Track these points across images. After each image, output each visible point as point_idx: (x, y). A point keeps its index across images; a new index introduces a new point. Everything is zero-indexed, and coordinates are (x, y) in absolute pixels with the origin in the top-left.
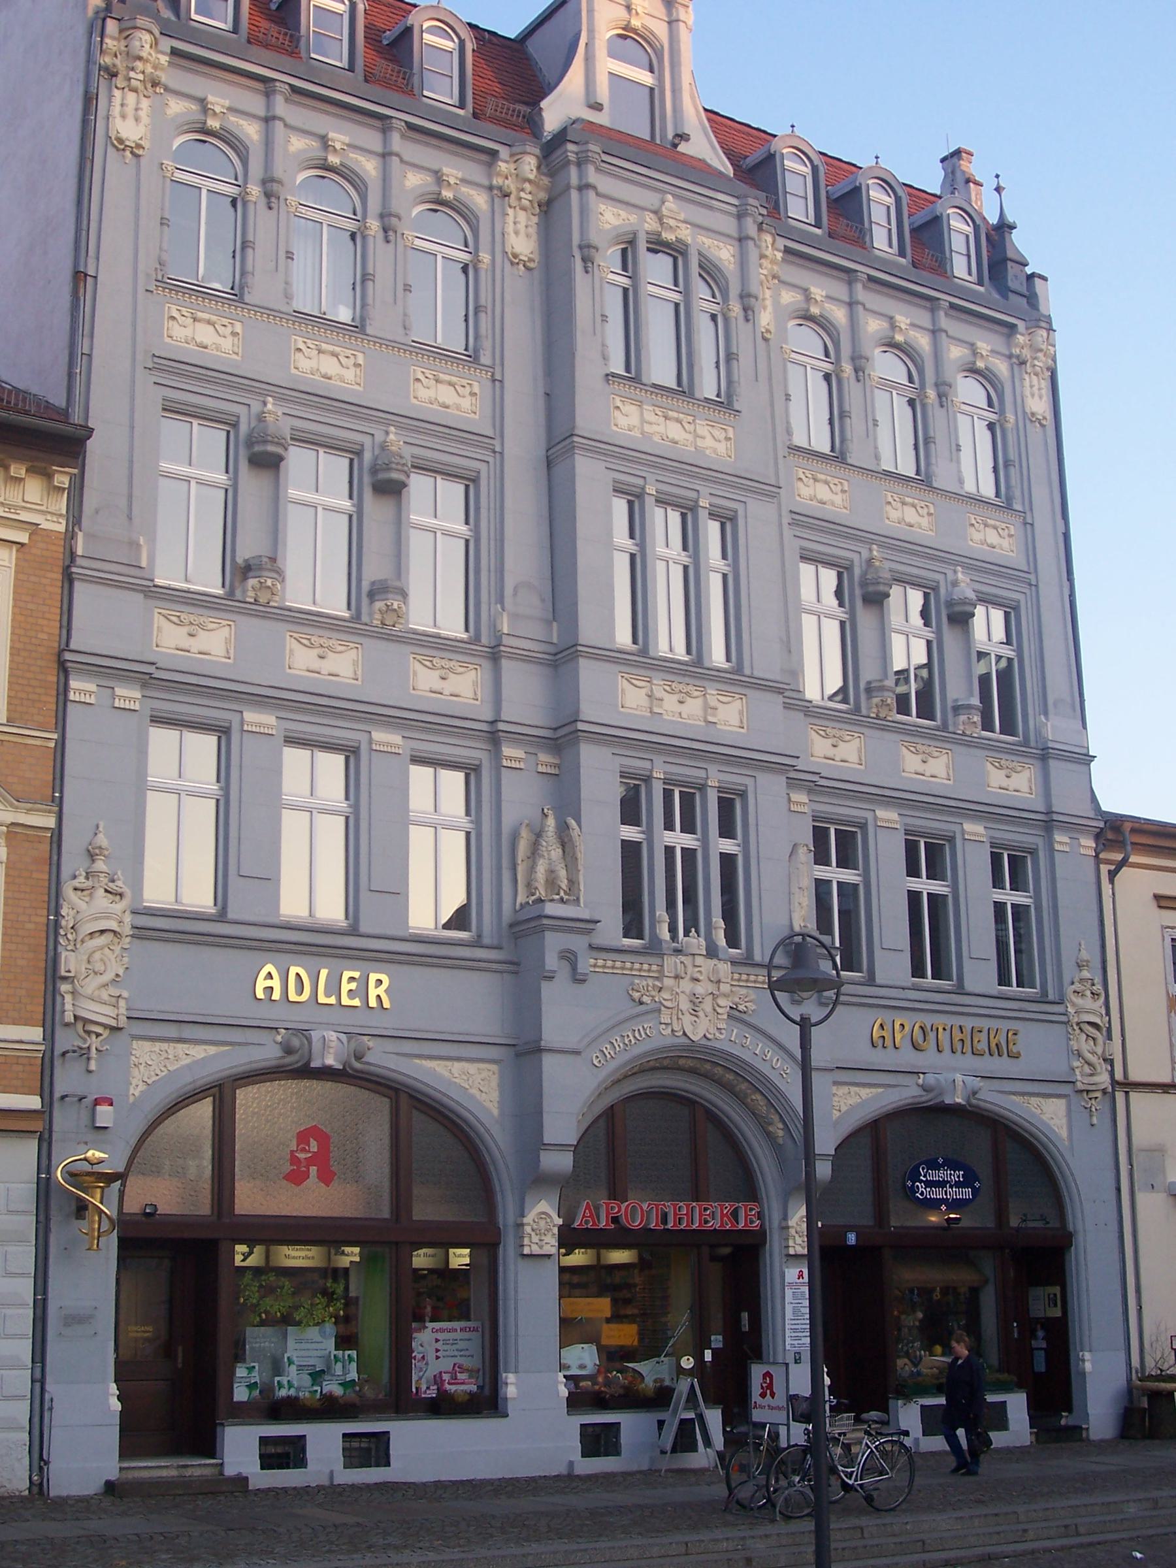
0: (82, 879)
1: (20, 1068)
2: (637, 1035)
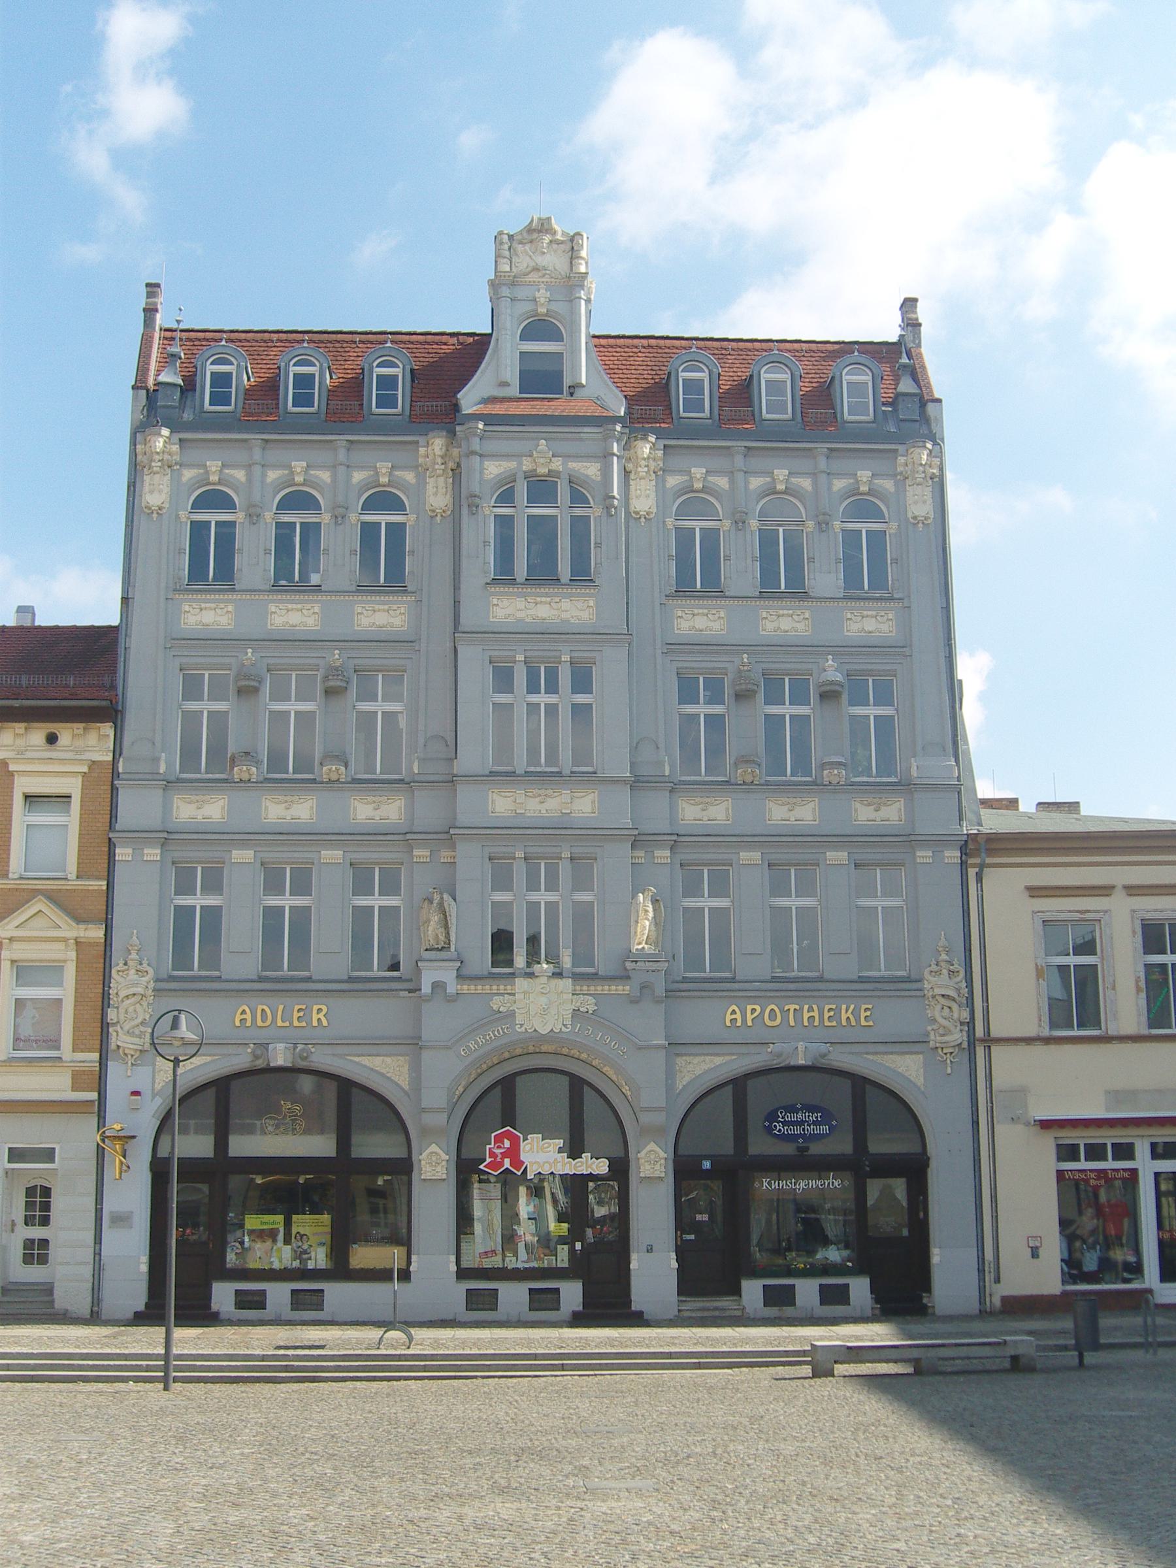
0: (121, 965)
1: (86, 1077)
2: (496, 1033)
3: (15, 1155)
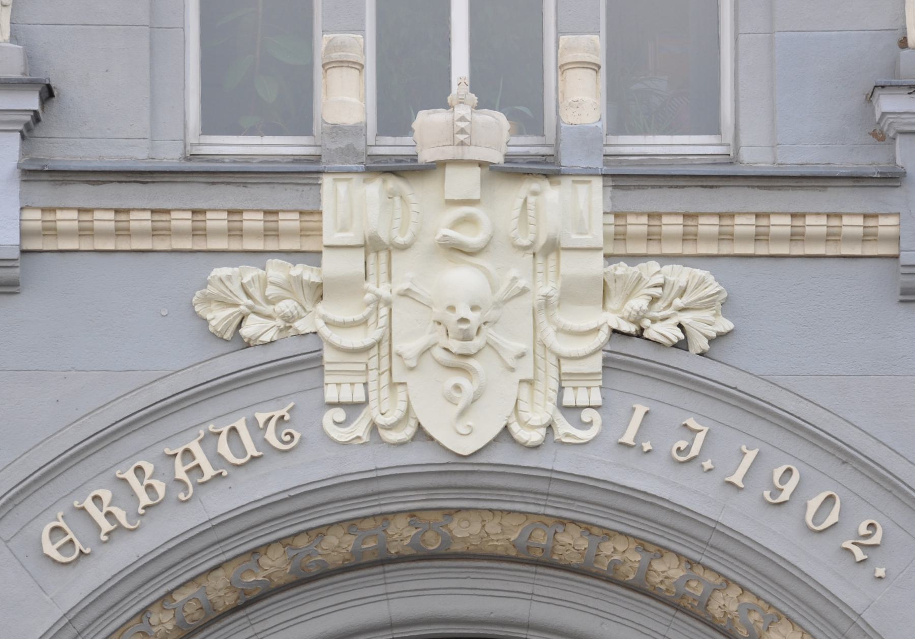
2: (223, 447)
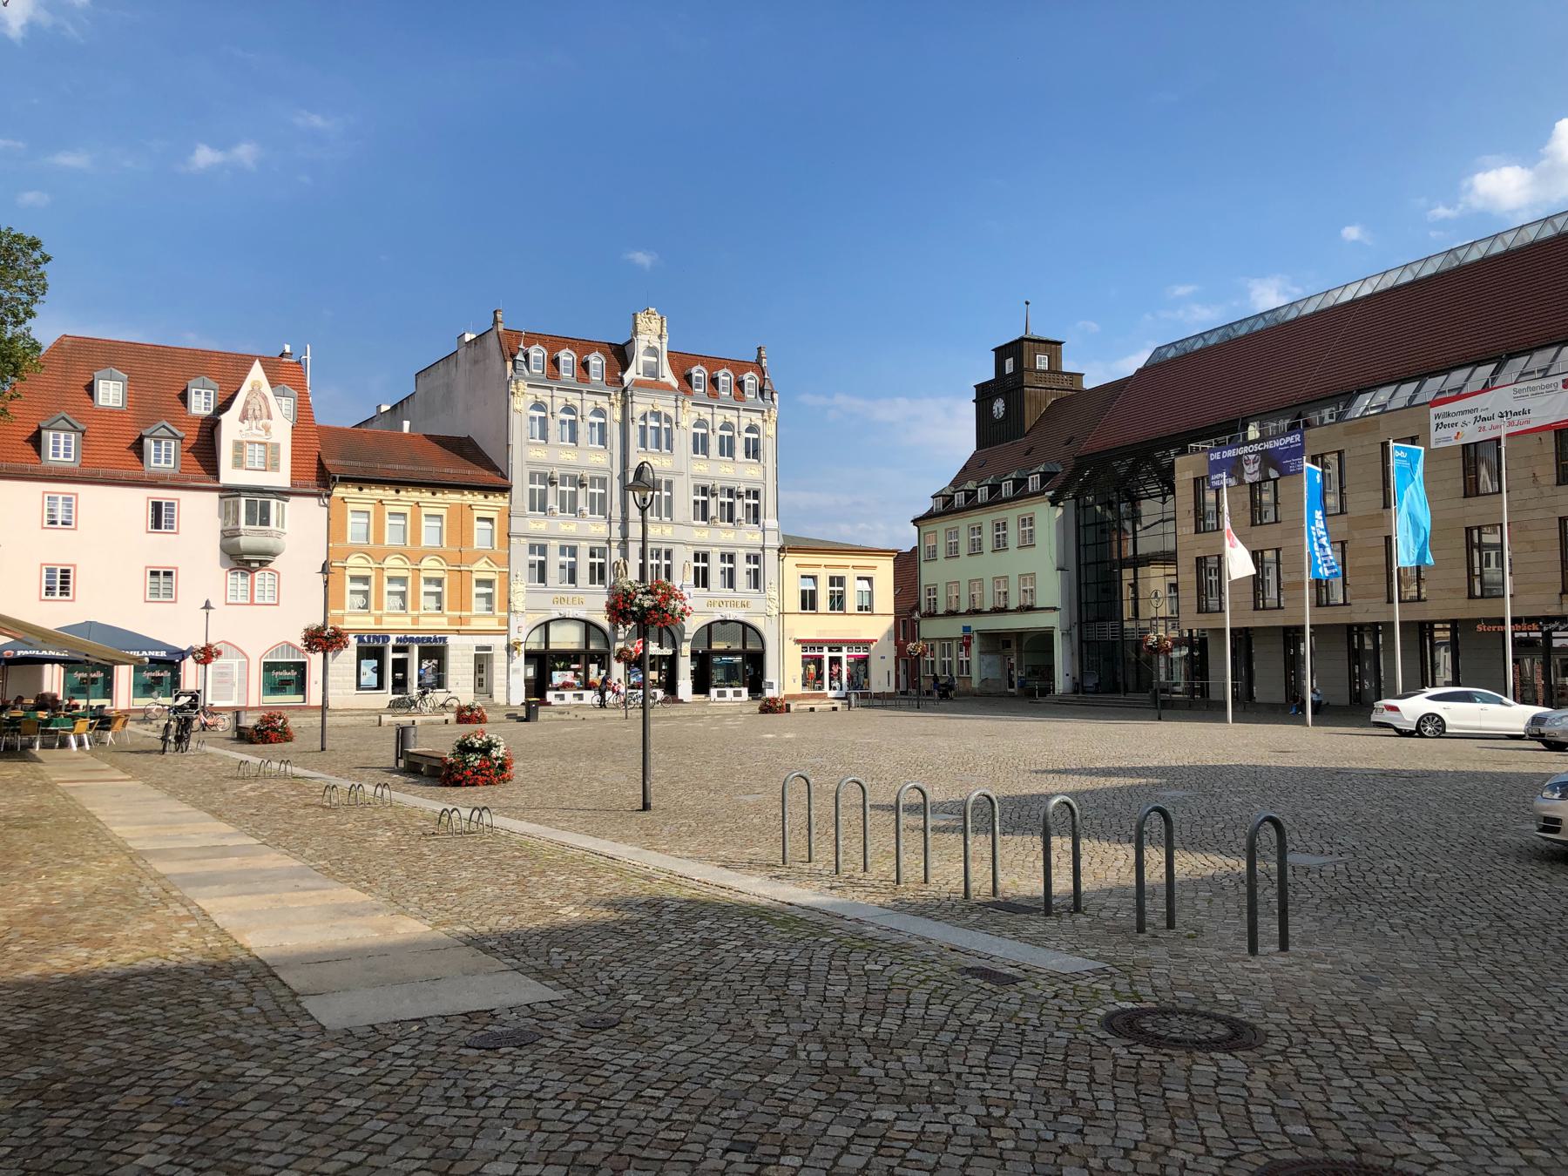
3: (478, 648)
